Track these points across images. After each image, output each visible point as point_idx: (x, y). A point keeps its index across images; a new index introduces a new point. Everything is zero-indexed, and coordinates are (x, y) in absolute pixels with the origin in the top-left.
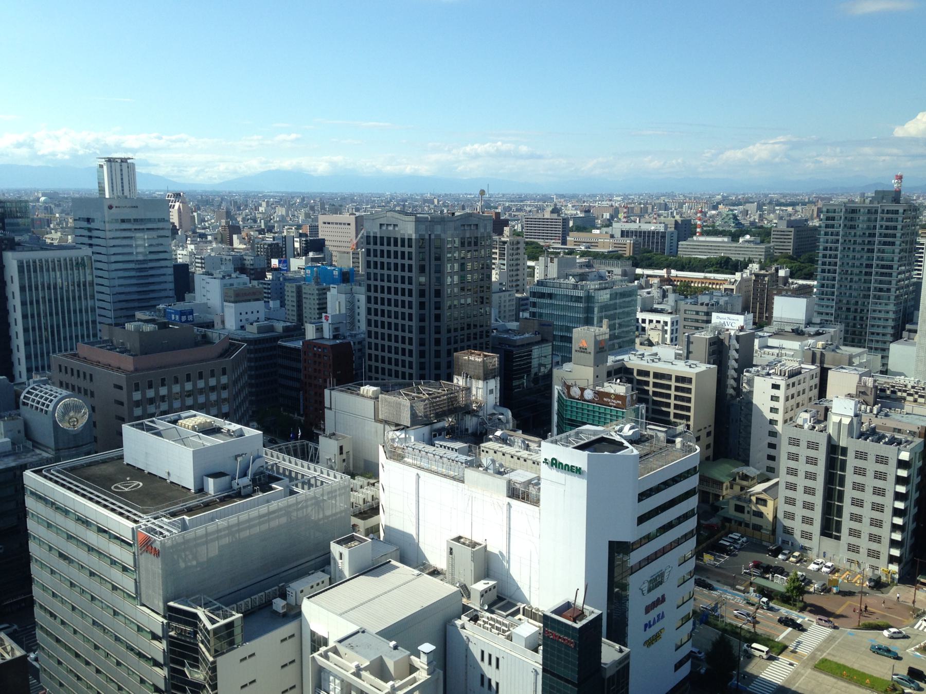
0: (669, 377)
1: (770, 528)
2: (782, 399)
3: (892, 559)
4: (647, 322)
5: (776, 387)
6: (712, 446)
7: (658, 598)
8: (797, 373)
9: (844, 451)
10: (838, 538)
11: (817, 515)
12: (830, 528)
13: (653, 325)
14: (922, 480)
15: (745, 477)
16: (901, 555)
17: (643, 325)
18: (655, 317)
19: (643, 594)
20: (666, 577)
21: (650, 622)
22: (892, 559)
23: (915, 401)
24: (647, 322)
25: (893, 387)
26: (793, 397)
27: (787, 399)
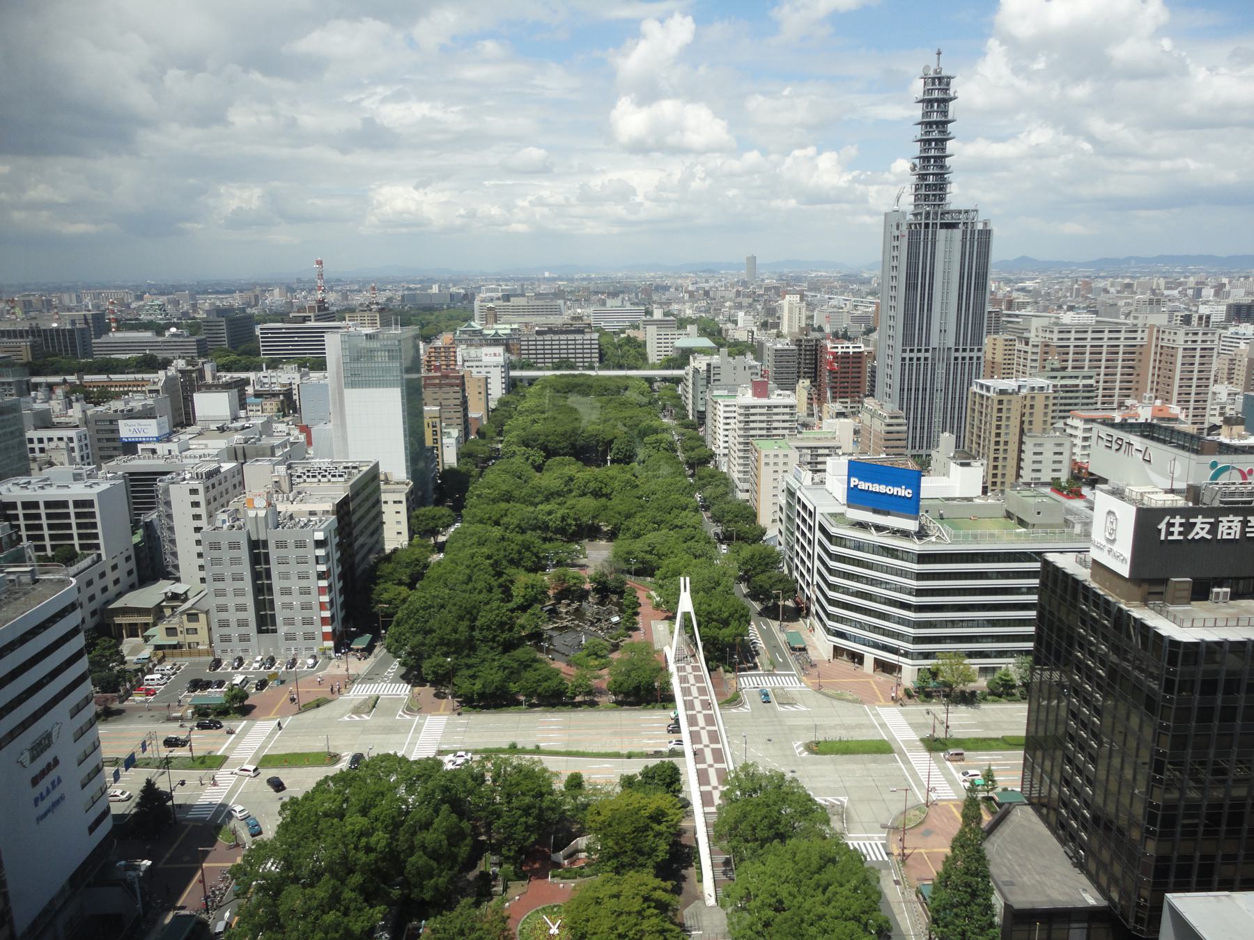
0: (64, 504)
1: (207, 641)
2: (203, 504)
3: (325, 636)
4: (45, 440)
5: (194, 491)
6: (135, 571)
7: (49, 764)
8: (217, 471)
9: (265, 544)
10: (275, 631)
11: (251, 615)
12: (265, 623)
13: (53, 445)
14: (342, 555)
15: (175, 597)
16: (334, 630)
17: (41, 445)
18: (55, 434)
19: (24, 766)
20: (54, 738)
21: (41, 794)
22: (325, 636)
23: (329, 481)
24: (45, 440)
25: (309, 471)
26: (215, 499)
27: (208, 503)
